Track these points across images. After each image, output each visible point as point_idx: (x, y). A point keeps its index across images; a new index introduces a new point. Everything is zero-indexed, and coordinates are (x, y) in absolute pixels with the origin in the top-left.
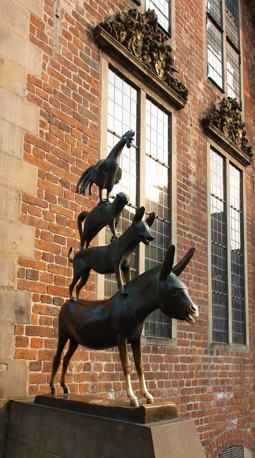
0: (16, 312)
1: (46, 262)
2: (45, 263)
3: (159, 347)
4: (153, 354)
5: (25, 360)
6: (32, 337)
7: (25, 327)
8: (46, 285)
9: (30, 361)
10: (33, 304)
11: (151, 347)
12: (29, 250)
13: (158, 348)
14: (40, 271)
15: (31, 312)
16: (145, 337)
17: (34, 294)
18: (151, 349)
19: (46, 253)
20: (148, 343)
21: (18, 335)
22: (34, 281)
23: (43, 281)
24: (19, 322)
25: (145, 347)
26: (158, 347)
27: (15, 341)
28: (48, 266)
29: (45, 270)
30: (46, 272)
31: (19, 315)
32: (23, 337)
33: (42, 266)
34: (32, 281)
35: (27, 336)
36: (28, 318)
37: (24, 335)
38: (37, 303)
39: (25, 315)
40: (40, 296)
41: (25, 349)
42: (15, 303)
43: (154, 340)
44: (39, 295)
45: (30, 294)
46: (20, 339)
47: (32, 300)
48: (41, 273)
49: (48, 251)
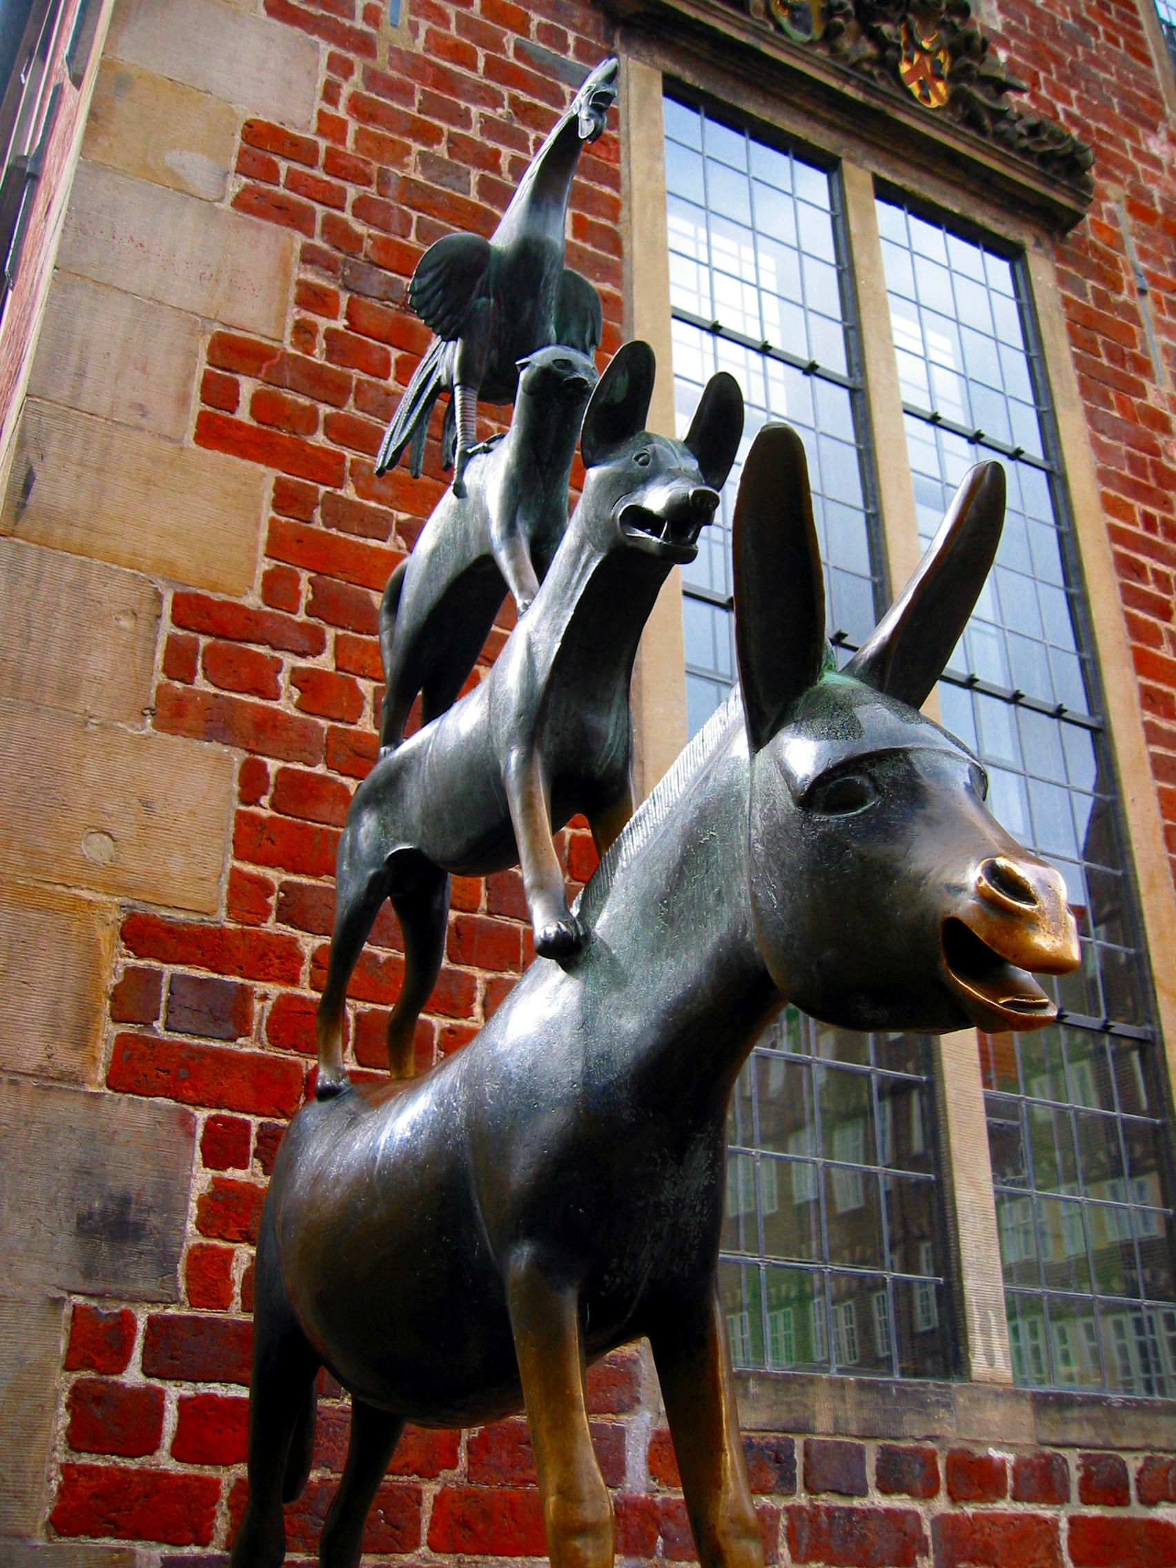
0: (87, 1227)
1: (298, 933)
2: (293, 941)
3: (1133, 1463)
4: (1094, 1511)
5: (123, 1543)
6: (188, 1390)
7: (141, 1325)
8: (296, 1065)
9: (166, 1550)
10: (201, 1179)
11: (1073, 1458)
12: (195, 873)
13: (1123, 1464)
14: (260, 987)
15: (191, 1227)
16: (1017, 1395)
17: (212, 1120)
18: (1075, 1475)
19: (300, 887)
20: (1044, 1436)
21: (89, 1374)
22: (216, 1044)
23: (275, 1041)
24: (99, 1286)
25: (1028, 1463)
26: (1125, 1457)
27: (62, 1410)
28: (314, 960)
29: (294, 981)
30: (297, 991)
31: (105, 1248)
32: (123, 1385)
33: (280, 962)
34: (203, 1042)
35: (156, 1382)
36: (166, 1263)
37: (133, 1376)
38: (232, 1173)
39: (145, 1245)
40: (254, 1130)
41: (132, 1464)
42: (84, 1171)
43: (1085, 1411)
44: (246, 1125)
45: (186, 1122)
46: (98, 1400)
47: (198, 1155)
48: (264, 997)
49: (316, 875)
